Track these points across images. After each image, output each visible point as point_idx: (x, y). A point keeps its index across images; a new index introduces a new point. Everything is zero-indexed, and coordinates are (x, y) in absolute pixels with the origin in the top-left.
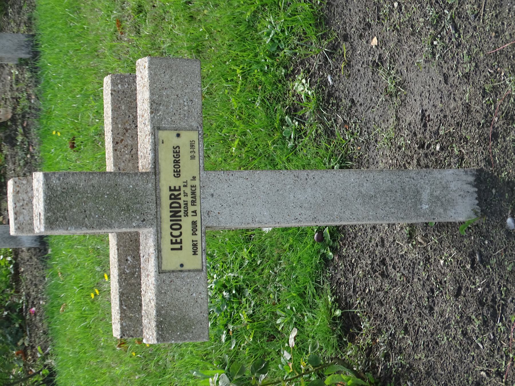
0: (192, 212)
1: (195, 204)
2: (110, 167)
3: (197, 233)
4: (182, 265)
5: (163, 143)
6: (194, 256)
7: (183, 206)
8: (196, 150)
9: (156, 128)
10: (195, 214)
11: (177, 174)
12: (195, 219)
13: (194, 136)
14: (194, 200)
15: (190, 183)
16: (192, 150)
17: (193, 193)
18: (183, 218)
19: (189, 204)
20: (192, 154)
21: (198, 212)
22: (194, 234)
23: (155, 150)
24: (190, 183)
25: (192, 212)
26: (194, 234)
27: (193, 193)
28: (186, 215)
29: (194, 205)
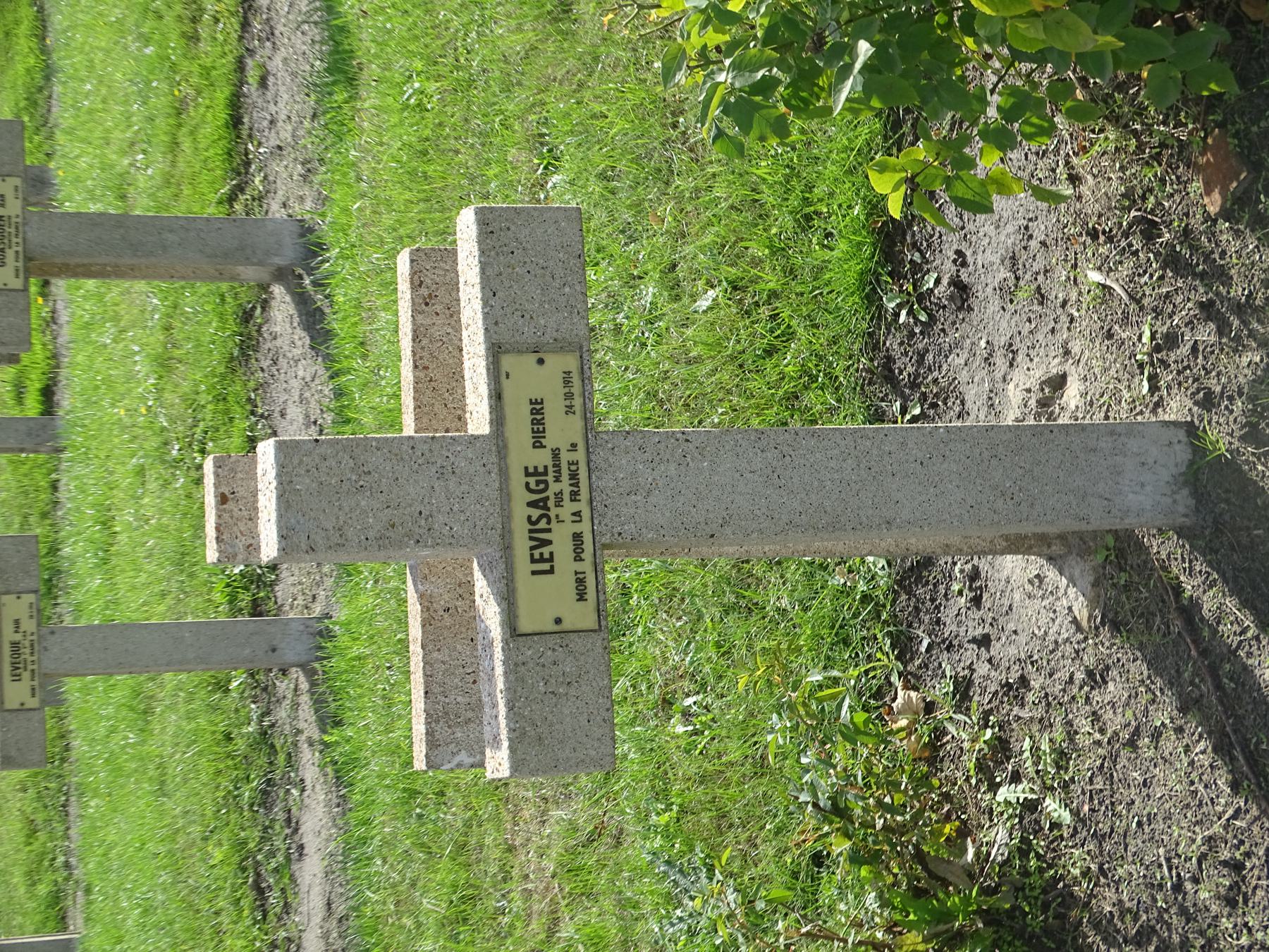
0: (574, 514)
2: (409, 429)
3: (583, 556)
4: (558, 621)
8: (577, 389)
9: (495, 351)
12: (577, 528)
13: (570, 362)
15: (565, 457)
16: (567, 390)
17: (574, 476)
19: (566, 496)
22: (578, 558)
23: (497, 397)
25: (574, 514)
27: (574, 476)
29: (575, 500)
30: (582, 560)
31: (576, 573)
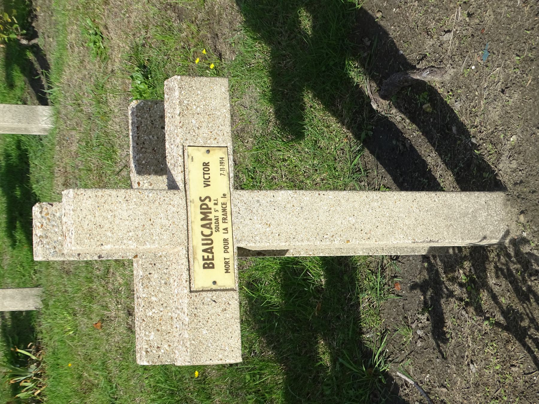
0: (224, 229)
1: (226, 221)
10: (226, 232)
12: (226, 236)
14: (225, 217)
15: (221, 200)
17: (224, 210)
19: (220, 221)
20: (222, 172)
21: (230, 230)
22: (226, 251)
24: (221, 200)
25: (224, 229)
27: (224, 210)
29: (225, 222)
31: (225, 259)
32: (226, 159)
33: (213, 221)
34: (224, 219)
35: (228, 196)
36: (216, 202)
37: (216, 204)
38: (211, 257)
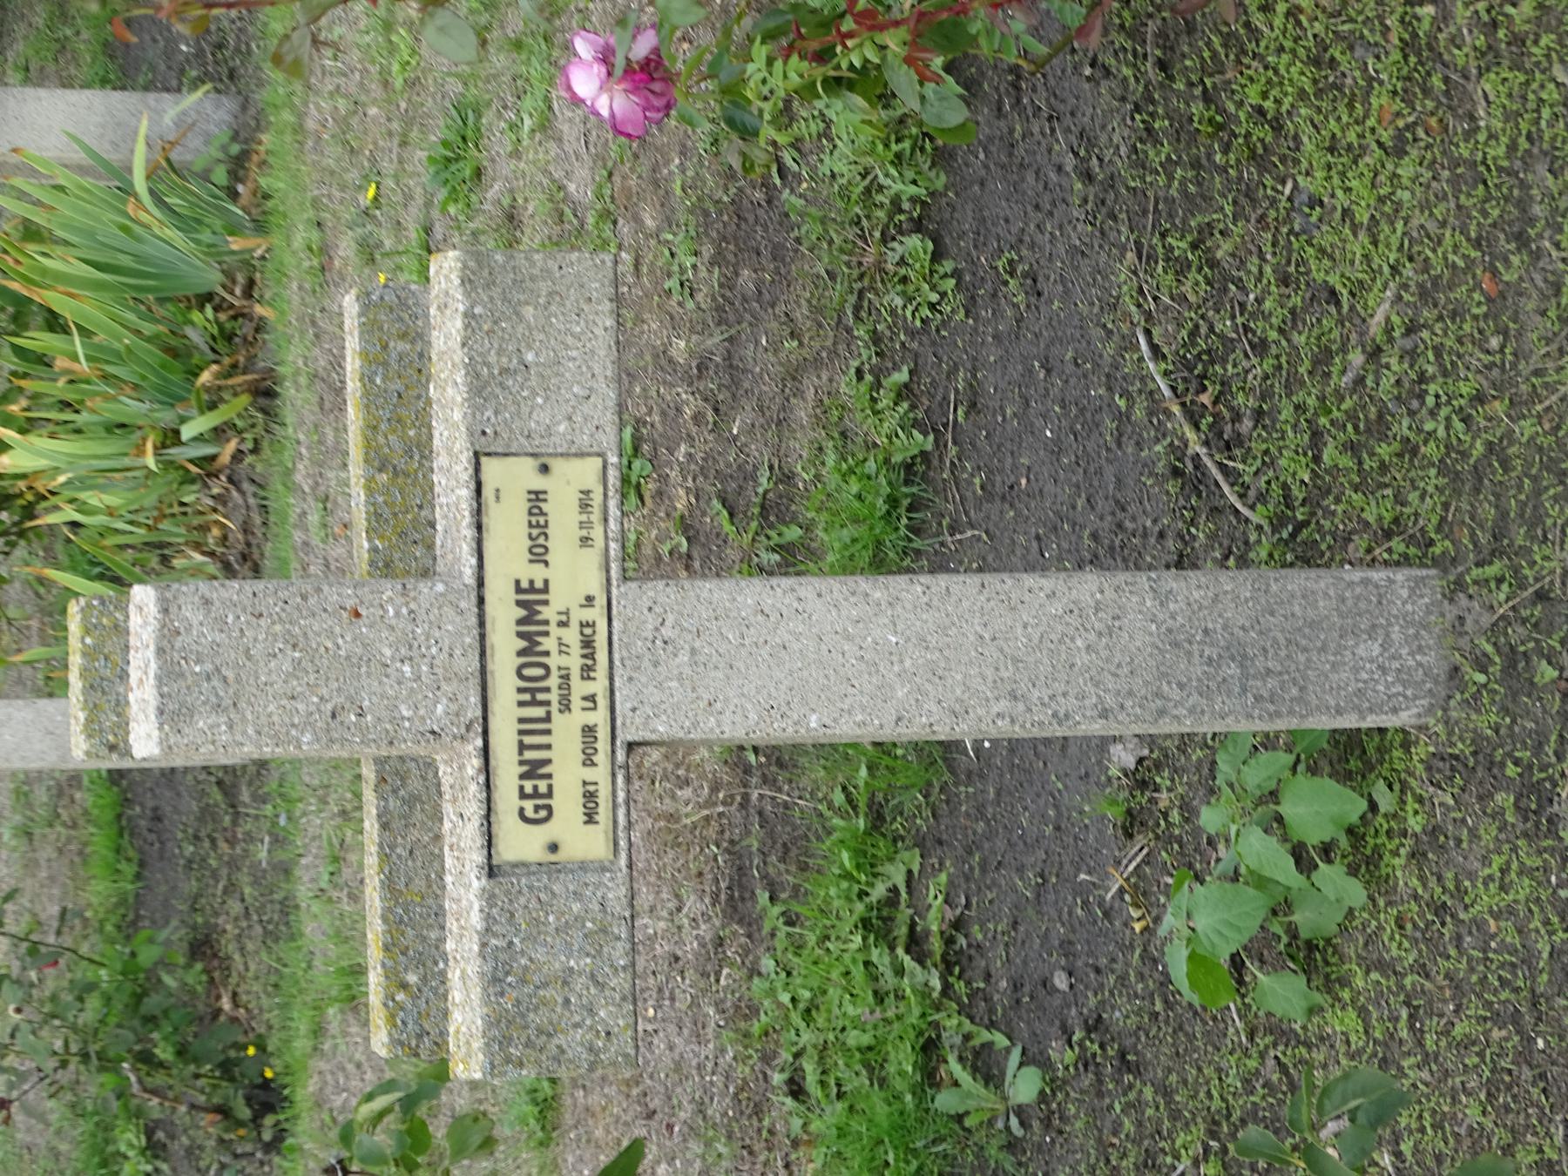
0: (585, 699)
3: (595, 759)
5: (498, 498)
6: (590, 827)
7: (553, 681)
11: (537, 808)
14: (590, 662)
16: (584, 518)
17: (588, 643)
18: (555, 714)
22: (589, 762)
24: (578, 615)
25: (585, 699)
26: (589, 762)
27: (588, 643)
28: (566, 707)
29: (589, 678)
30: (594, 764)
31: (585, 783)
32: (597, 497)
33: (555, 673)
34: (587, 672)
35: (601, 601)
36: (564, 618)
37: (562, 624)
38: (543, 788)
